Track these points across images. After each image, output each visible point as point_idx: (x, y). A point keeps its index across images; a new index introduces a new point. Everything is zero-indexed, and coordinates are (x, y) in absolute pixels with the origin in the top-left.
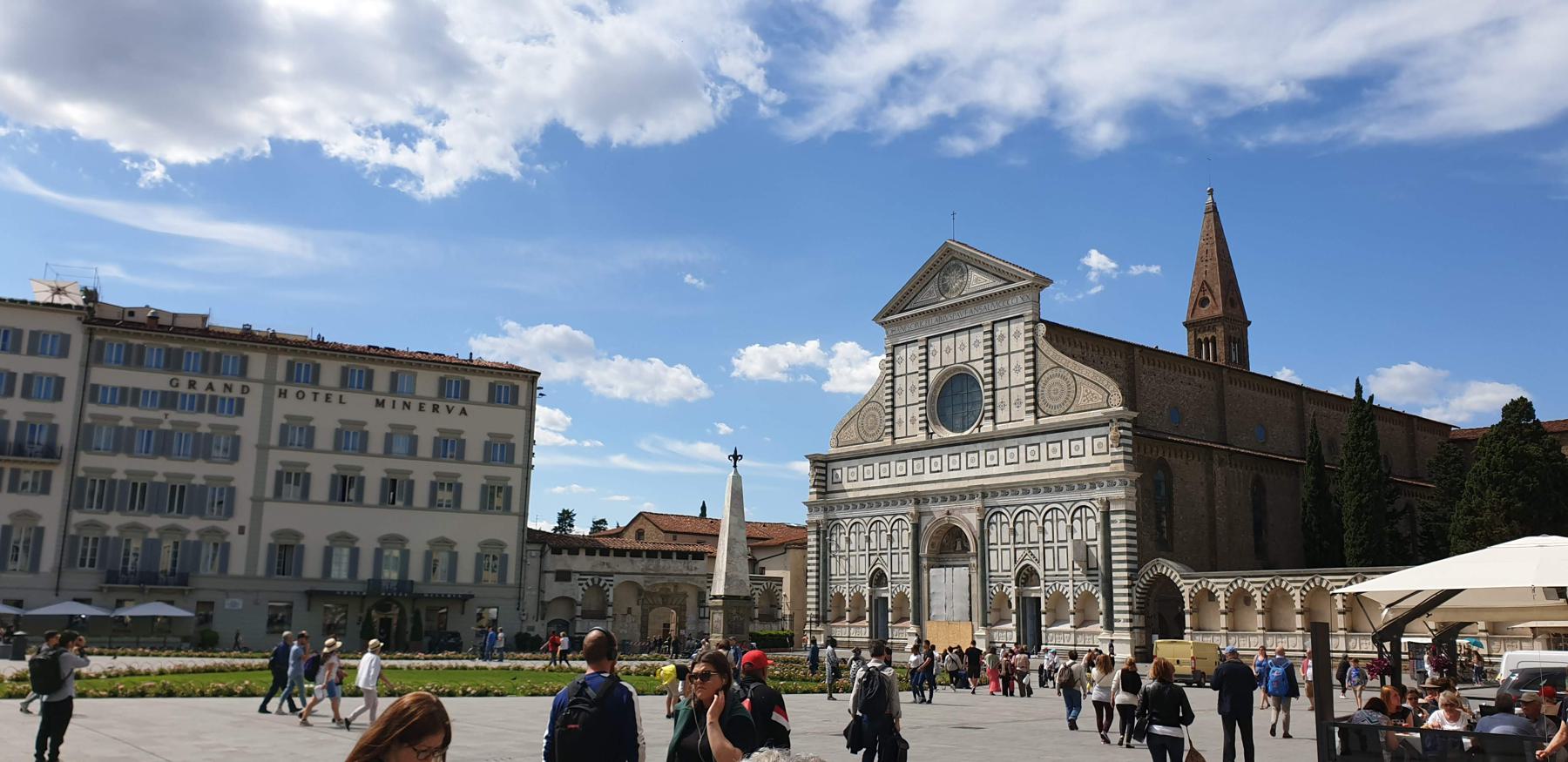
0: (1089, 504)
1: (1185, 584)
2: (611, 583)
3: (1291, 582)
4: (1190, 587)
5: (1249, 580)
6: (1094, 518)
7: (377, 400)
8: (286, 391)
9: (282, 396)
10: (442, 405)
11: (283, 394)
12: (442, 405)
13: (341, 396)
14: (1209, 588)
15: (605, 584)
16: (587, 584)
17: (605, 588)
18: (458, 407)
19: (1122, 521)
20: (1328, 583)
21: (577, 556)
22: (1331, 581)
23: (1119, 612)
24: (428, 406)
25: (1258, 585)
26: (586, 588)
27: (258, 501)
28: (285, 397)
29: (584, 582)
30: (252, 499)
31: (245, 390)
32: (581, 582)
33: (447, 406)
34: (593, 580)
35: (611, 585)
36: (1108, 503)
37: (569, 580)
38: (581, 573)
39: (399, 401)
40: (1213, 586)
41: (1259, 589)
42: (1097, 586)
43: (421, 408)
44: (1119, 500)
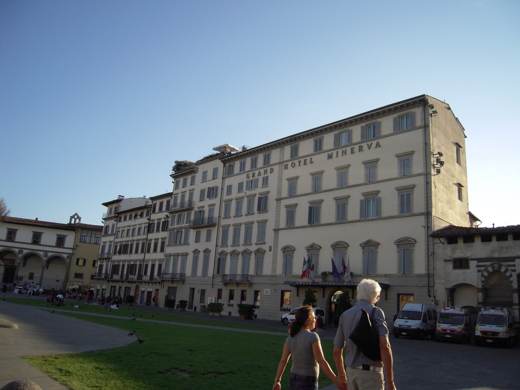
2: (513, 268)
7: (329, 154)
8: (287, 164)
9: (286, 168)
10: (365, 145)
11: (286, 167)
12: (365, 145)
13: (311, 159)
15: (507, 270)
16: (486, 270)
17: (508, 274)
18: (374, 143)
21: (474, 244)
24: (357, 148)
26: (486, 274)
27: (276, 231)
28: (287, 169)
29: (483, 268)
30: (274, 230)
31: (272, 171)
32: (480, 269)
33: (368, 145)
34: (492, 266)
35: (514, 271)
37: (467, 267)
38: (479, 260)
39: (340, 151)
43: (352, 152)
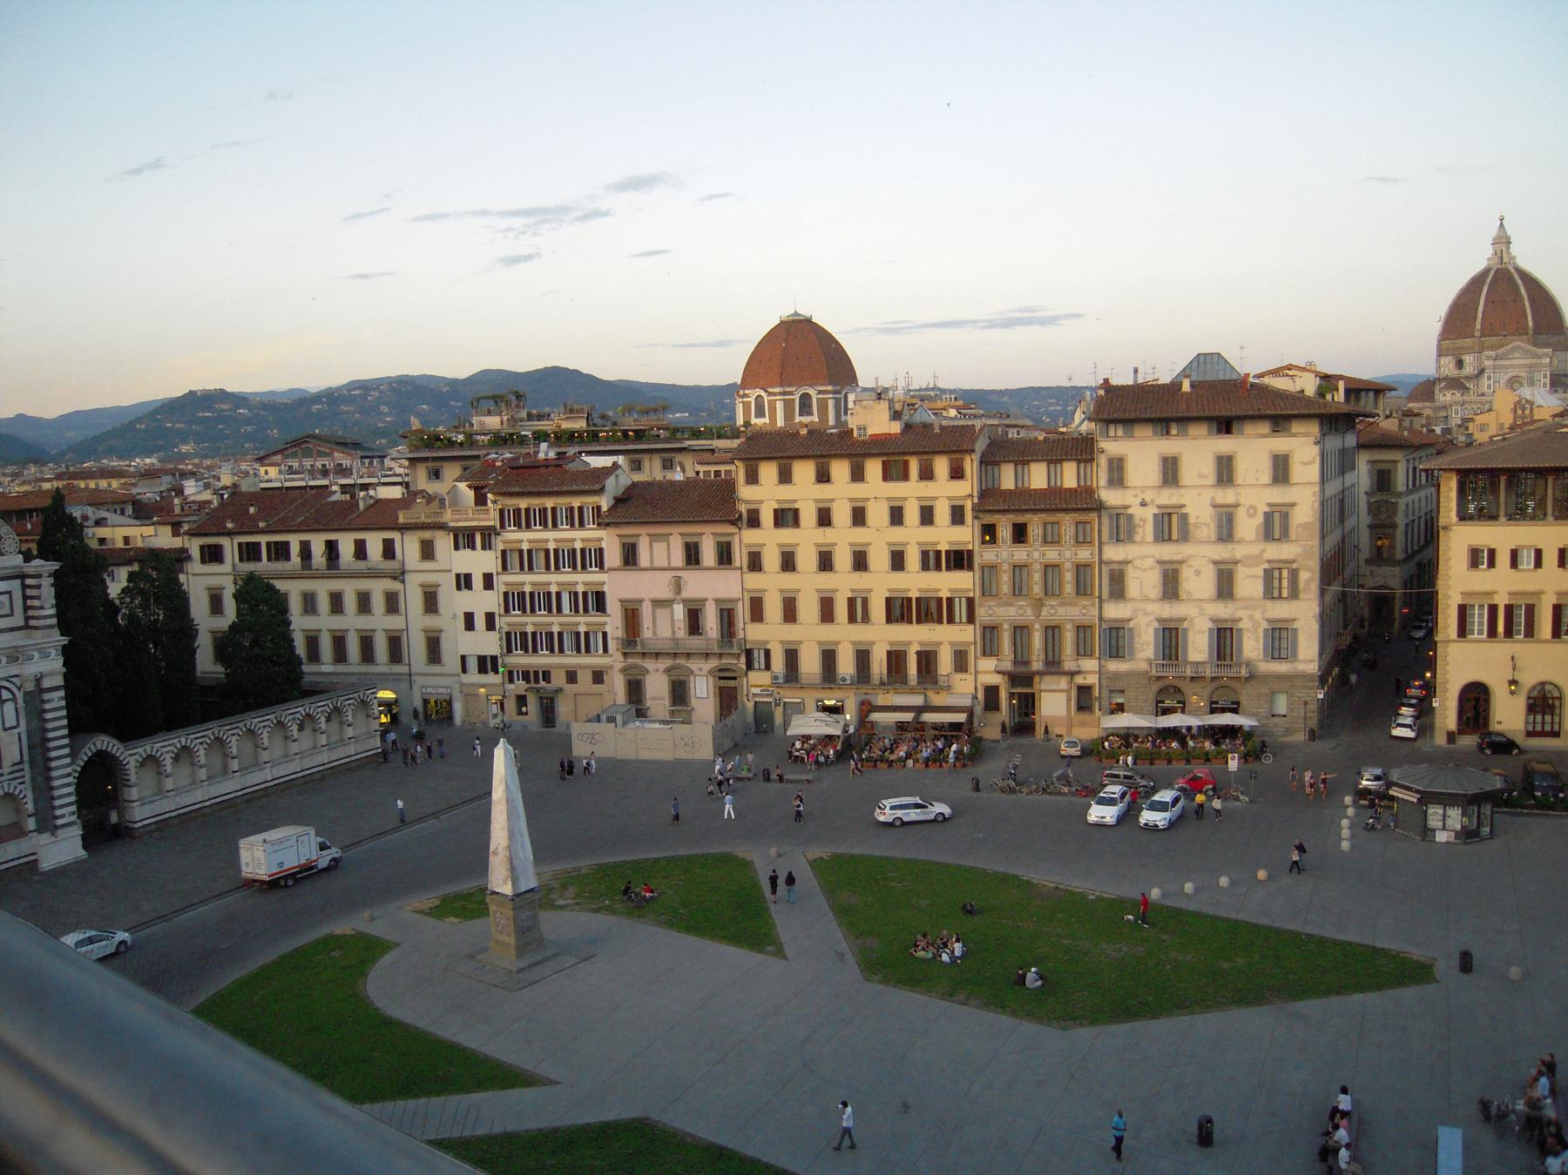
0: (6, 684)
1: (130, 755)
3: (228, 730)
4: (136, 757)
5: (193, 736)
6: (14, 699)
14: (154, 754)
19: (49, 701)
20: (256, 725)
22: (260, 722)
23: (62, 806)
25: (200, 740)
36: (38, 680)
40: (157, 751)
41: (201, 743)
42: (23, 783)
44: (51, 674)
